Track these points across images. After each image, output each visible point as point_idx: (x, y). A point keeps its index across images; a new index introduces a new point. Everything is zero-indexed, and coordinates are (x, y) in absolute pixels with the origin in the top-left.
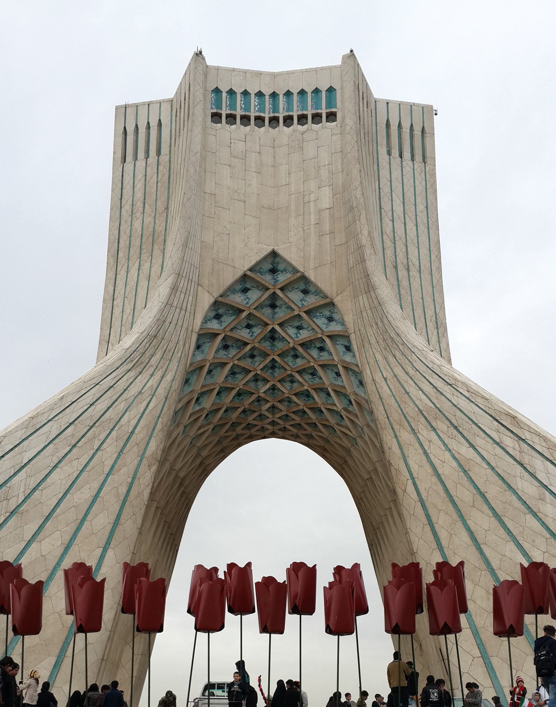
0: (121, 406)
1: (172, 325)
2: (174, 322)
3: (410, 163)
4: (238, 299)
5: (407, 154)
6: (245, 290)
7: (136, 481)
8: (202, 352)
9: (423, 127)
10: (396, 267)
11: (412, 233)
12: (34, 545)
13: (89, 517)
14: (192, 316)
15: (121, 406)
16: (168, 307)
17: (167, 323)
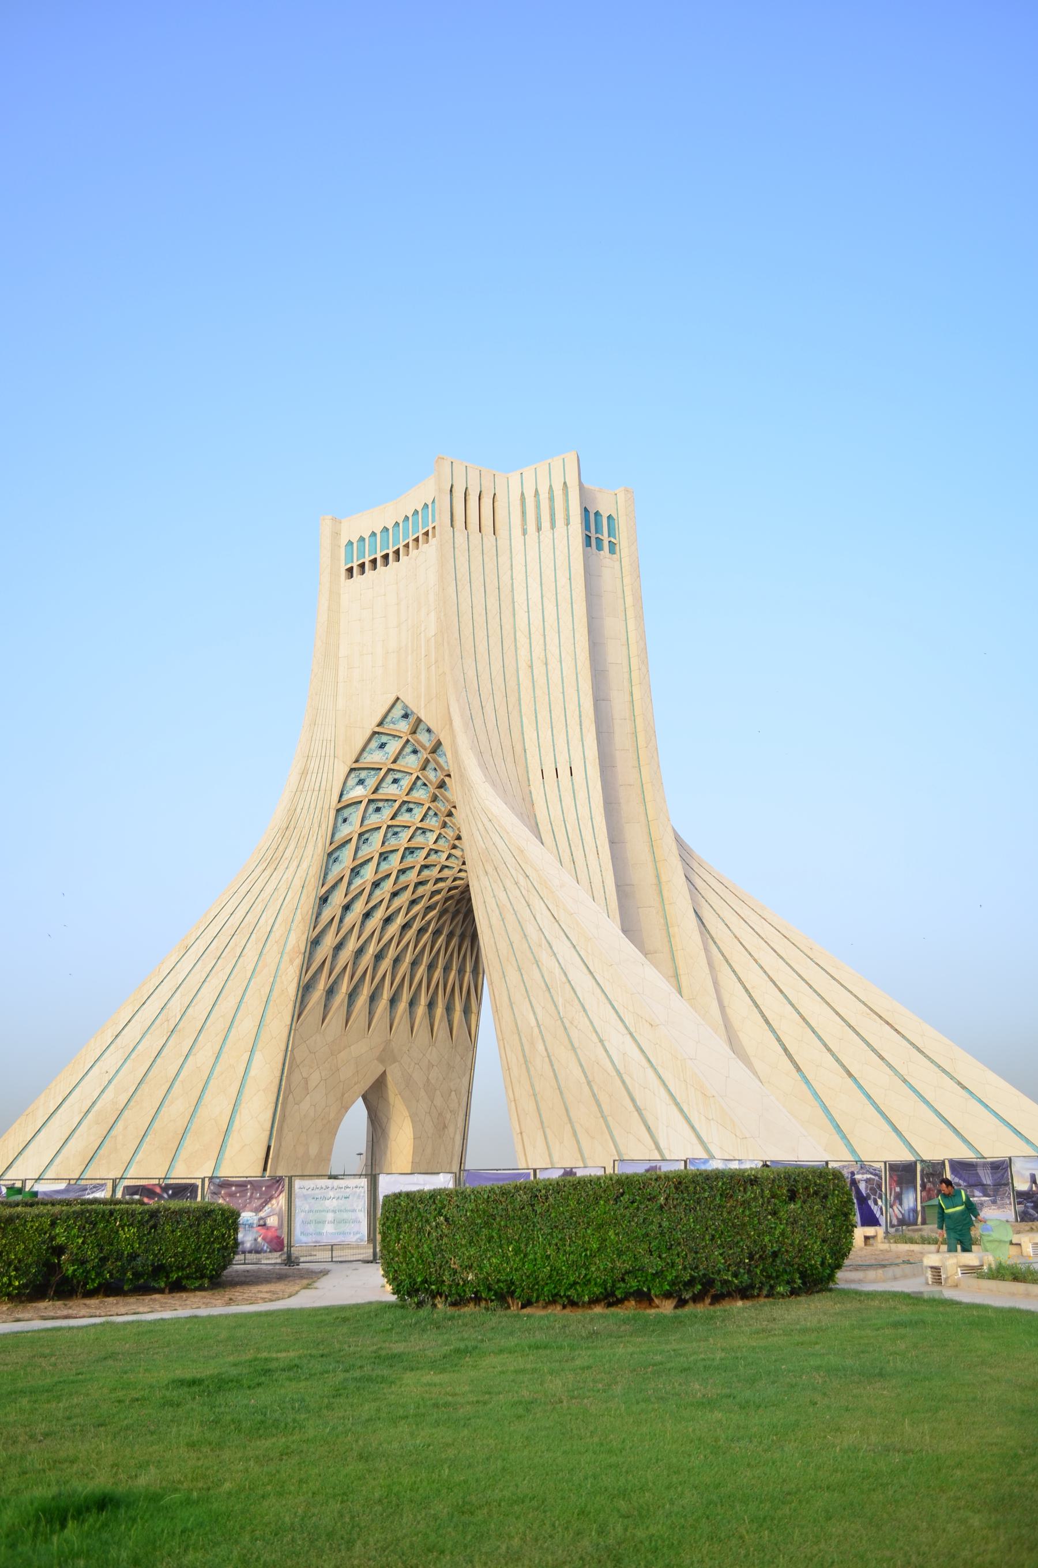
0: (258, 908)
1: (305, 811)
2: (306, 807)
3: (549, 534)
4: (375, 757)
5: (546, 524)
6: (382, 746)
7: (278, 979)
8: (351, 824)
9: (565, 483)
10: (531, 667)
11: (551, 619)
12: (191, 1059)
13: (236, 1023)
14: (329, 792)
15: (258, 908)
16: (298, 793)
17: (298, 810)
